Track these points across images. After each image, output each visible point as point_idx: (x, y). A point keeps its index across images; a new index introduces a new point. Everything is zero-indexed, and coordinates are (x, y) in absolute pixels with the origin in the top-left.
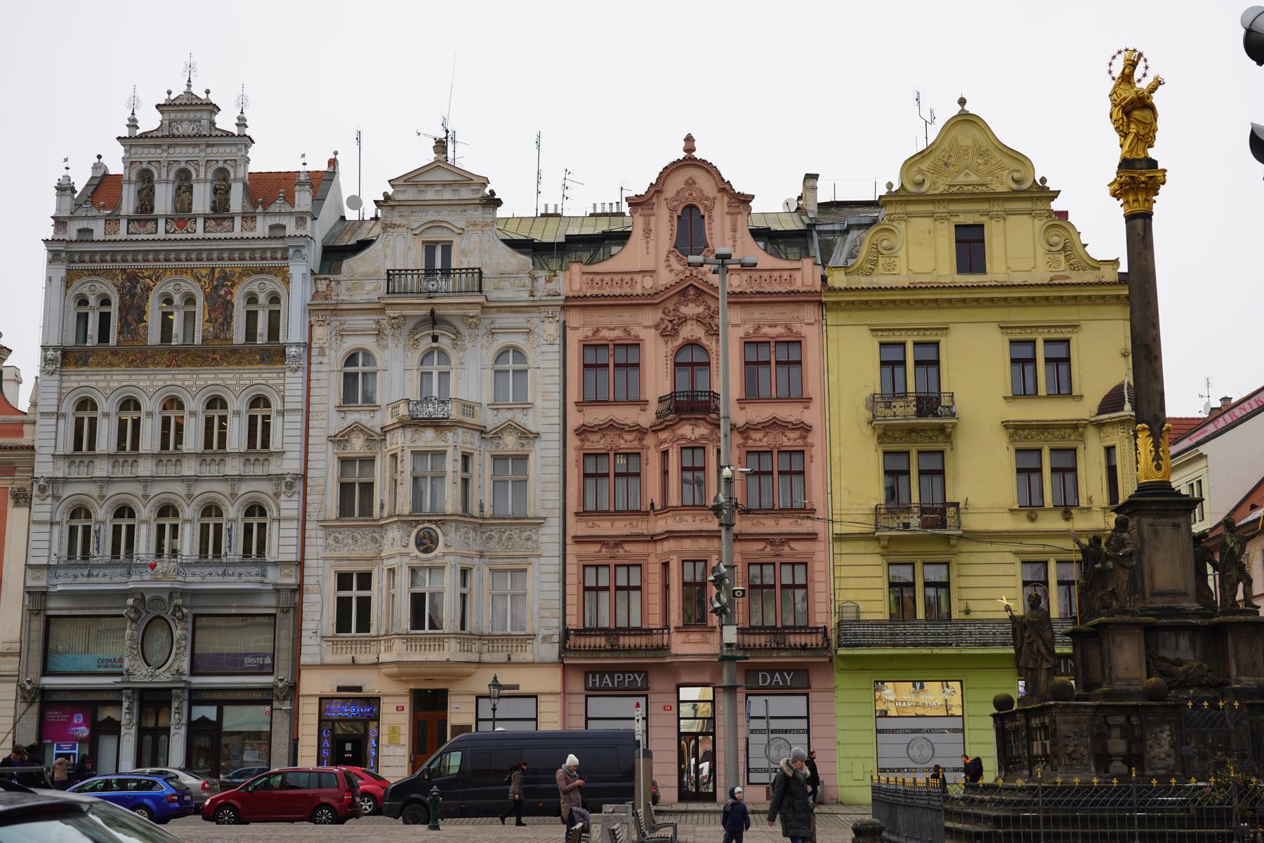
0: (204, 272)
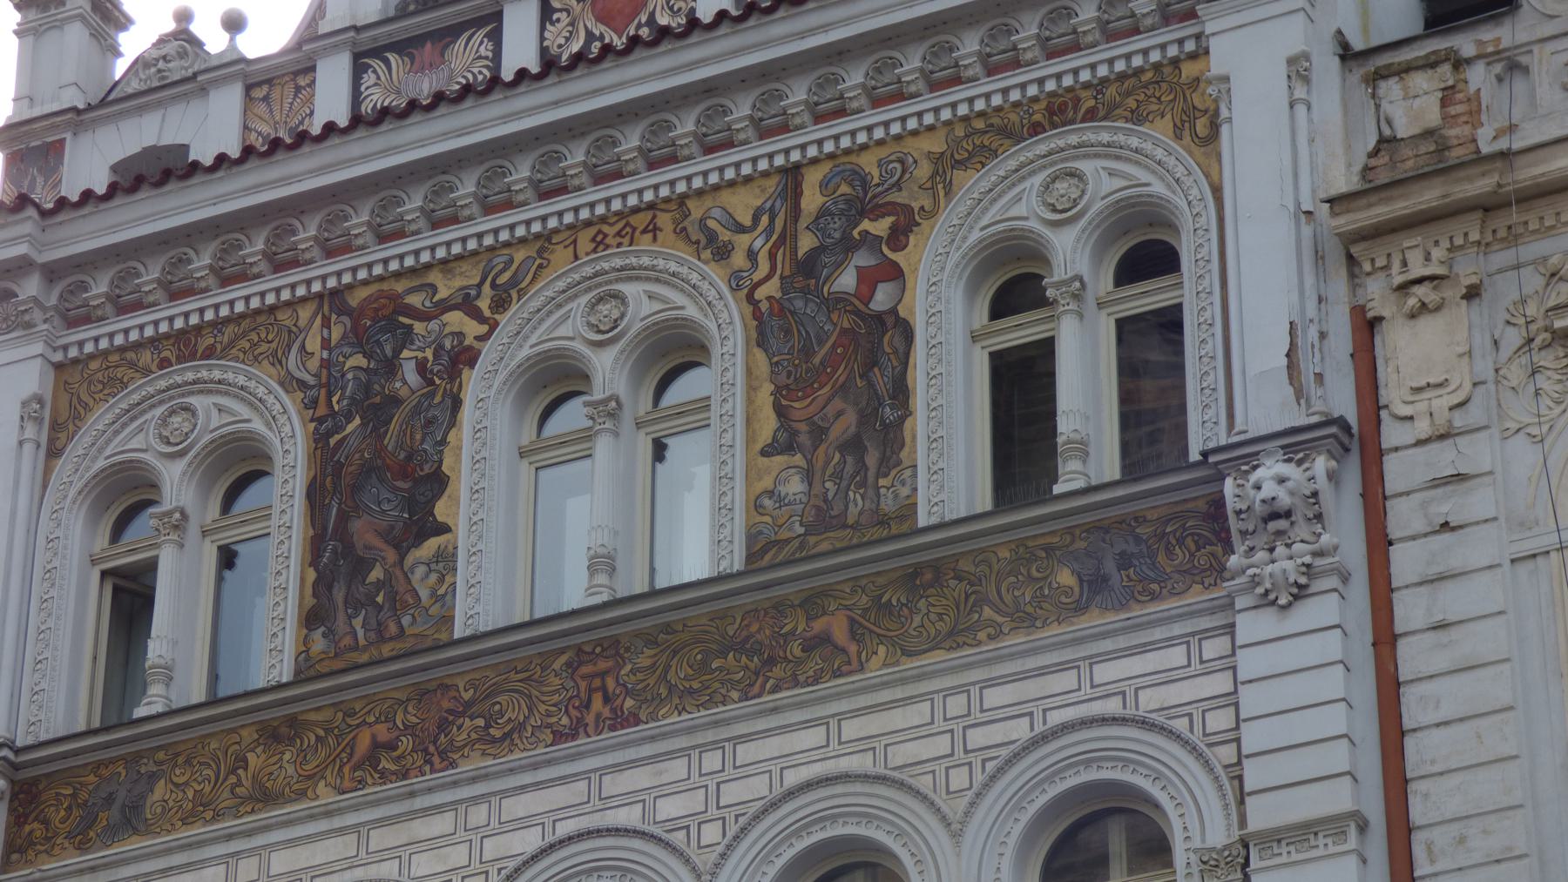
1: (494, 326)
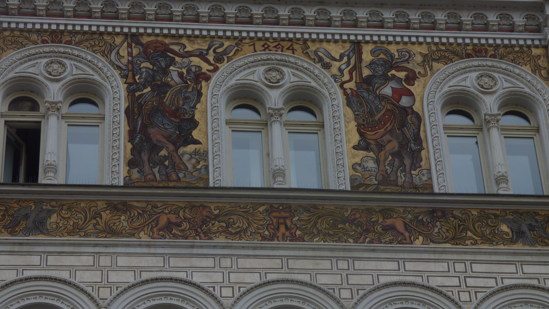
0: (336, 50)
1: (216, 69)
